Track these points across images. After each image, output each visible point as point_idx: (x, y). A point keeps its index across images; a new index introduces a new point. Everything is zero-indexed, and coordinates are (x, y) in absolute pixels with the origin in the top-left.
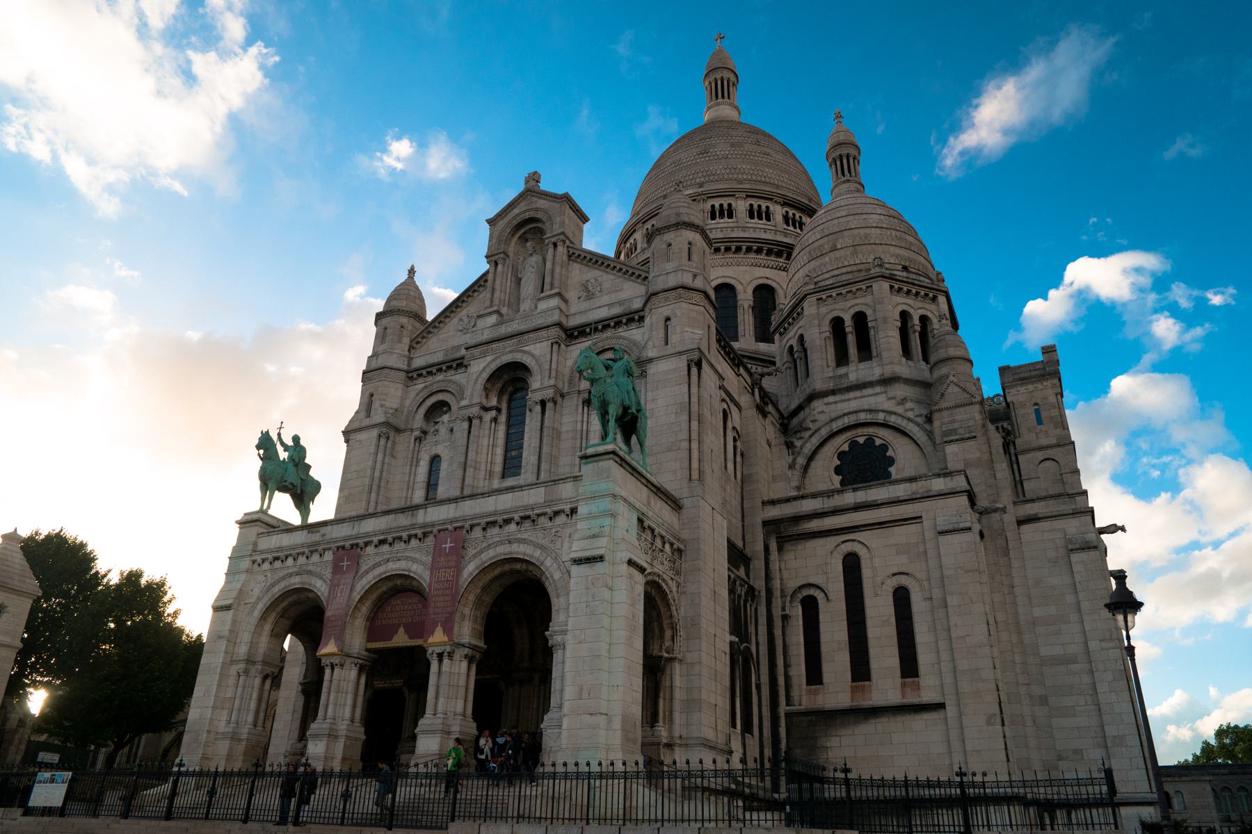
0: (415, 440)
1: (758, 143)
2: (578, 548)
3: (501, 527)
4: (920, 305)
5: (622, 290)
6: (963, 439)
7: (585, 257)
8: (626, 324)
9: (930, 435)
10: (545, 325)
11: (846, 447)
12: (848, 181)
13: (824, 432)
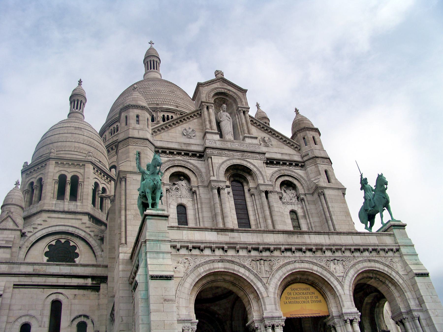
0: (166, 191)
3: (362, 252)
5: (283, 148)
7: (259, 125)
8: (294, 166)
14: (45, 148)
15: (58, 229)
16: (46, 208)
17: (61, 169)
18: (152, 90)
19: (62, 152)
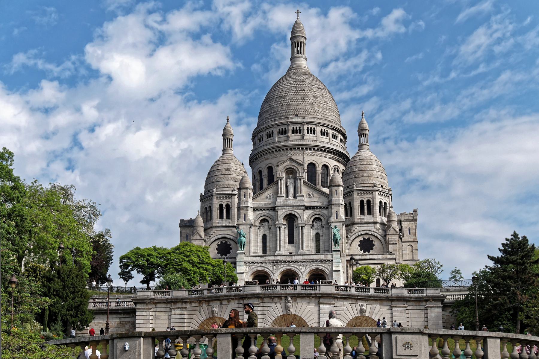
1: (322, 96)
2: (334, 269)
4: (385, 199)
6: (394, 244)
9: (385, 239)
10: (301, 205)
11: (362, 239)
12: (365, 145)
13: (357, 235)
14: (210, 185)
15: (221, 236)
16: (214, 225)
17: (220, 201)
18: (287, 99)
19: (219, 190)
